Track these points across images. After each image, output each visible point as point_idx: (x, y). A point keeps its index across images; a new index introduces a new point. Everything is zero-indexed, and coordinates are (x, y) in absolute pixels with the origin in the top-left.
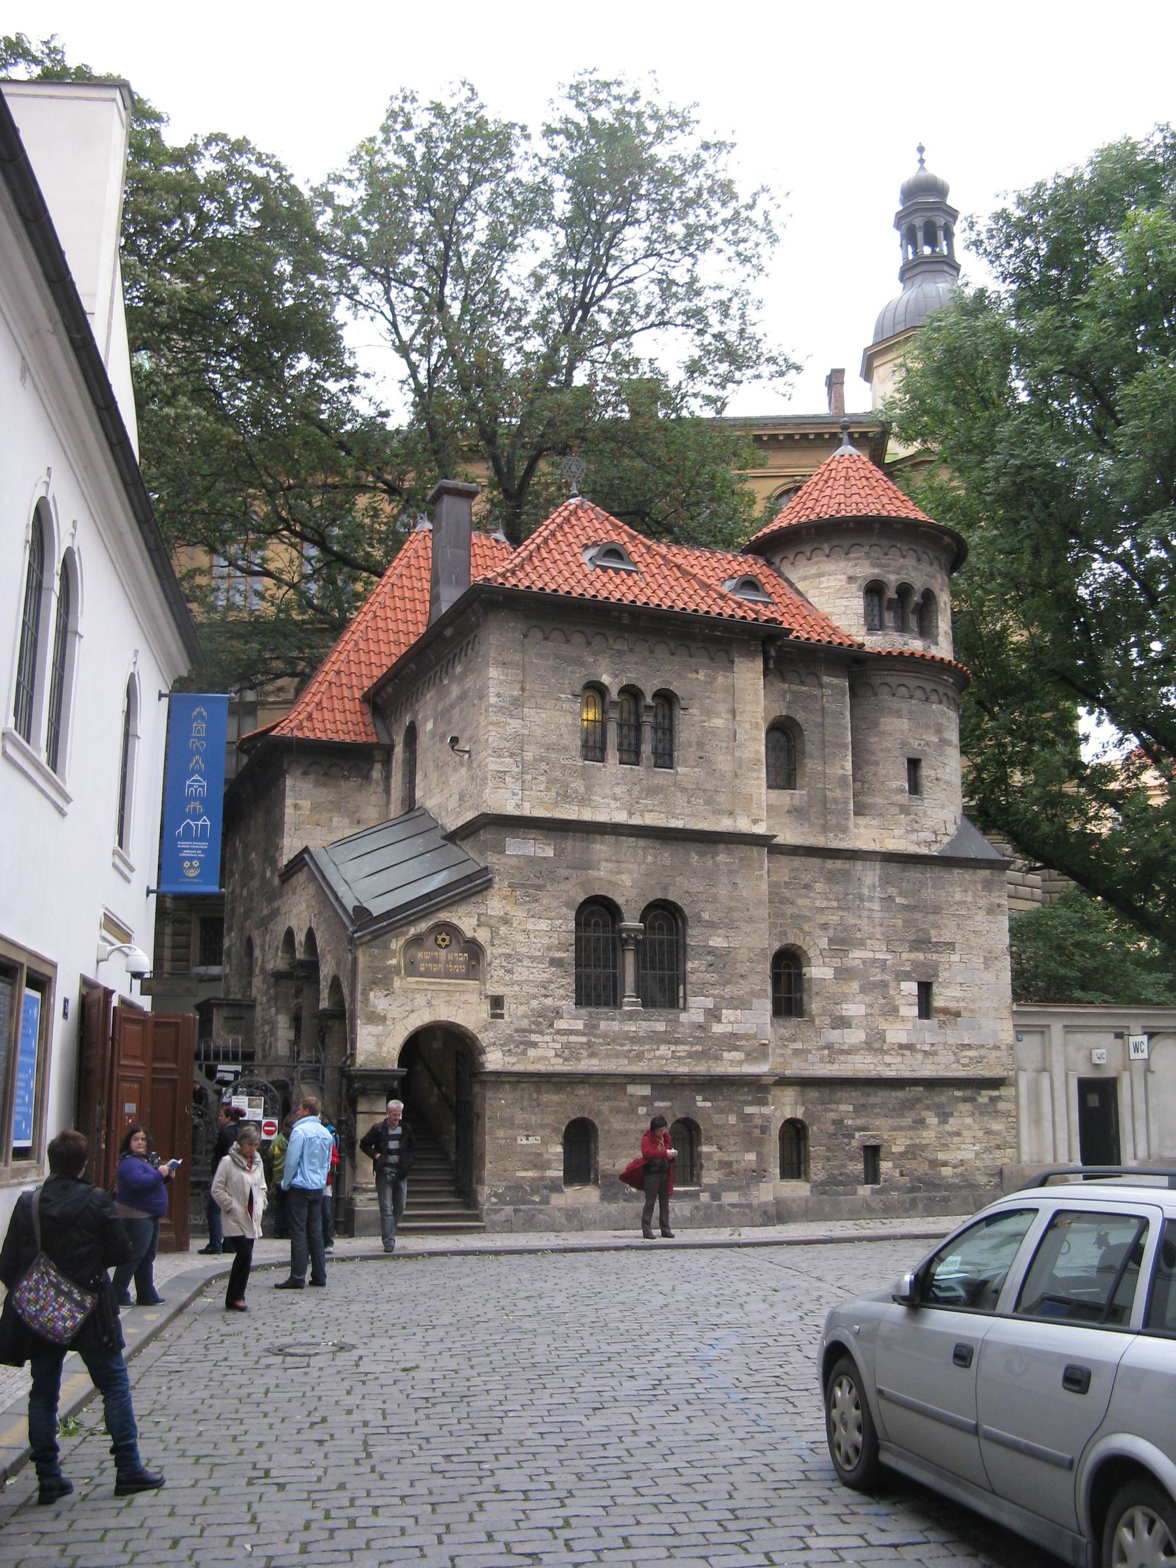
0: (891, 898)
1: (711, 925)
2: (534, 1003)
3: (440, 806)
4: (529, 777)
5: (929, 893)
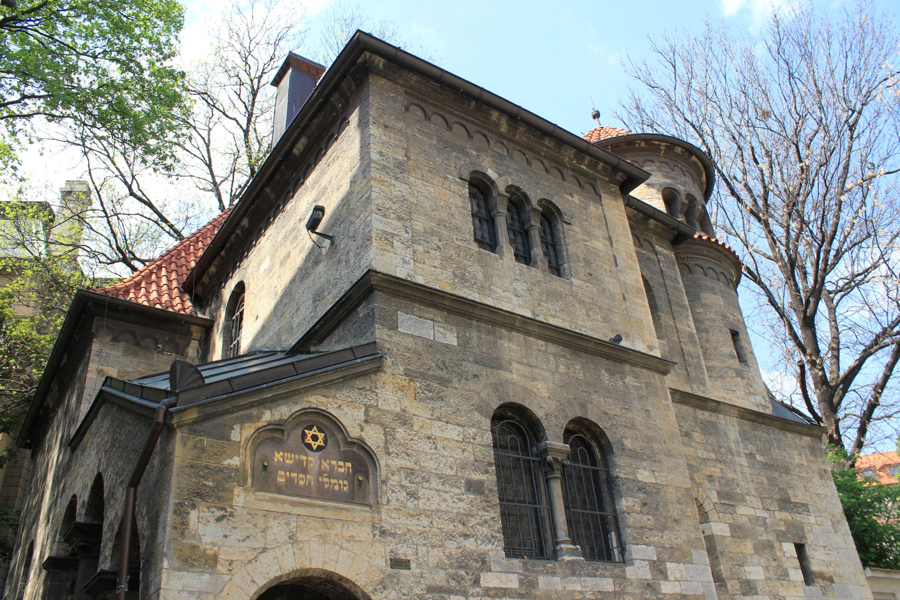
1: (635, 455)
3: (279, 334)
4: (420, 248)
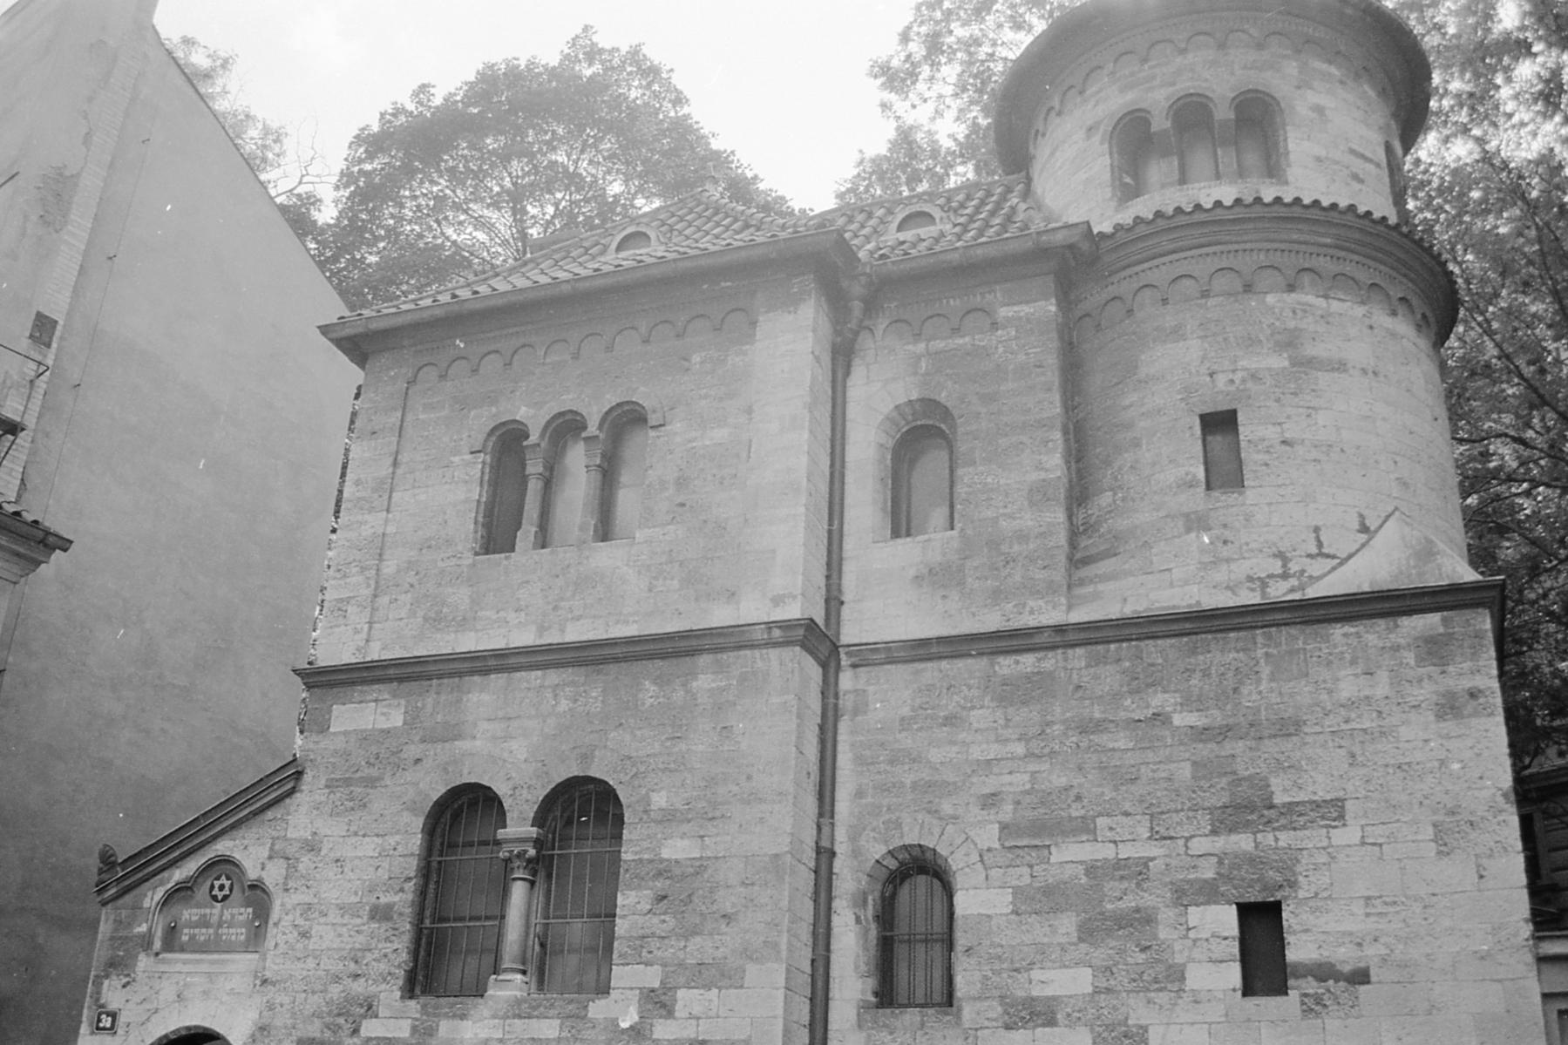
0: (1160, 718)
1: (669, 817)
2: (335, 991)
5: (1262, 694)
